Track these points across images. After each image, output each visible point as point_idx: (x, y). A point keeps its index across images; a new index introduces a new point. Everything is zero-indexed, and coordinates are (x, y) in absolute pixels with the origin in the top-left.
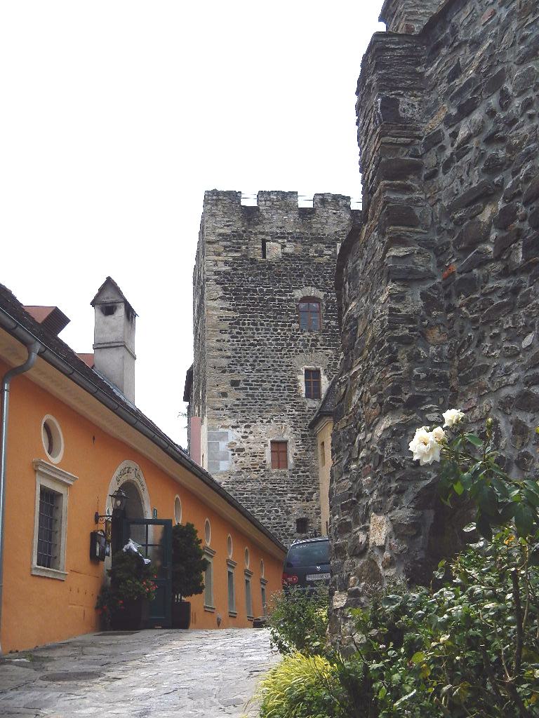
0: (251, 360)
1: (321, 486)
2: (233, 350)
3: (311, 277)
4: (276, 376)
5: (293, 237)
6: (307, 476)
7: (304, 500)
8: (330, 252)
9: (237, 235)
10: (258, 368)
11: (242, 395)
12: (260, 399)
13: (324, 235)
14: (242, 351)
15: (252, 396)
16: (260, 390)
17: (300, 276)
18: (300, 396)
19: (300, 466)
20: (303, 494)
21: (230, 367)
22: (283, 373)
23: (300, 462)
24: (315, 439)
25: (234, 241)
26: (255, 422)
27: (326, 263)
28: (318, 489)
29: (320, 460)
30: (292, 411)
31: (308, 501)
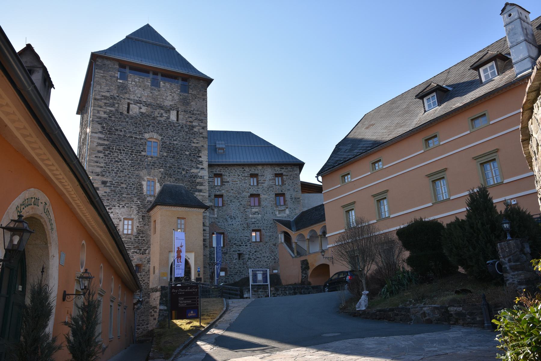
0: (115, 170)
1: (151, 246)
2: (105, 163)
3: (154, 127)
4: (130, 181)
5: (146, 104)
6: (144, 240)
7: (141, 254)
8: (166, 115)
9: (113, 98)
10: (119, 175)
11: (108, 190)
12: (119, 193)
13: (164, 105)
14: (110, 164)
15: (114, 191)
16: (119, 188)
17: (148, 126)
18: (143, 194)
19: (140, 234)
20: (140, 250)
21: (102, 173)
22: (134, 179)
23: (141, 232)
24: (150, 219)
25: (111, 101)
26: (115, 206)
27: (164, 121)
28: (150, 247)
29: (152, 230)
30: (137, 202)
31: (143, 254)
